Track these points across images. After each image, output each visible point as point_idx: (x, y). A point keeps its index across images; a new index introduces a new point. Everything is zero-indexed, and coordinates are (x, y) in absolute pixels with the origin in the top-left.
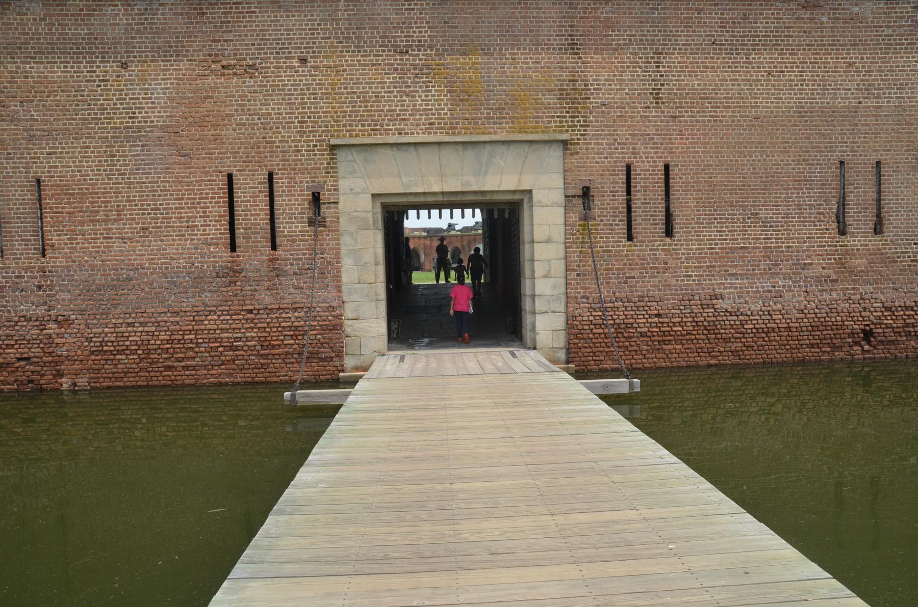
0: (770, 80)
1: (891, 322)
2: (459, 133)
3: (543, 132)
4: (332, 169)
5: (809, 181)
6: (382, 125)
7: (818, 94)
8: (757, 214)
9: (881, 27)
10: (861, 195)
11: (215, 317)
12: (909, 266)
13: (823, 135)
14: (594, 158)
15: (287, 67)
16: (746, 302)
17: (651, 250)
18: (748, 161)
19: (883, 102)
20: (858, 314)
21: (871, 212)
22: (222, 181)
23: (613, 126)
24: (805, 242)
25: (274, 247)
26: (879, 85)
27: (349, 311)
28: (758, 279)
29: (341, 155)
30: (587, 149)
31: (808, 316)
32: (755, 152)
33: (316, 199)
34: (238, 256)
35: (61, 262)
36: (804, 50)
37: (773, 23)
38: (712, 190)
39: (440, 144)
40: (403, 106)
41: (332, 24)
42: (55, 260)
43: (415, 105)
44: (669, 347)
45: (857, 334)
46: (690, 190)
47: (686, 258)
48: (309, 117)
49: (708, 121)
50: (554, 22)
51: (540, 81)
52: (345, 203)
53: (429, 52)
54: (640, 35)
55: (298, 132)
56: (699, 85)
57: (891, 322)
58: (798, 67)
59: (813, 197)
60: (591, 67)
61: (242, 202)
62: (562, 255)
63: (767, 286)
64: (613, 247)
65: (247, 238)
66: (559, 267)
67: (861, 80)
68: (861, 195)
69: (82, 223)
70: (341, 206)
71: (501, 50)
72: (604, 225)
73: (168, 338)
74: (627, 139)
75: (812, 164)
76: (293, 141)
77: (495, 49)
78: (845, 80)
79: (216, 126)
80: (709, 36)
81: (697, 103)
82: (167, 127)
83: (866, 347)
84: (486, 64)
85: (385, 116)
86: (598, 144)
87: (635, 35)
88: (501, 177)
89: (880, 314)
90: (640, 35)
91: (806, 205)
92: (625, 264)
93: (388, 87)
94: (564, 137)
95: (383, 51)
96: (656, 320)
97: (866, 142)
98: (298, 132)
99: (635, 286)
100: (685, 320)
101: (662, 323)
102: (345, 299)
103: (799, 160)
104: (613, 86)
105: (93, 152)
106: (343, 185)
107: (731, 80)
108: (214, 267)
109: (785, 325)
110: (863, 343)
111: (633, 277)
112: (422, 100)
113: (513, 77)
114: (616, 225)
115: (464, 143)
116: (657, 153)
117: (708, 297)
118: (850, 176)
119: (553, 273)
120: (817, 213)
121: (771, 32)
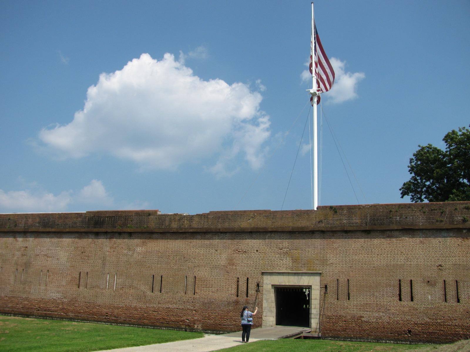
0: (378, 257)
1: (417, 328)
2: (294, 270)
3: (315, 270)
5: (389, 285)
6: (275, 268)
7: (392, 260)
8: (374, 294)
9: (411, 242)
10: (406, 289)
11: (232, 313)
12: (422, 311)
13: (394, 272)
14: (328, 277)
15: (253, 252)
16: (371, 319)
17: (343, 303)
18: (371, 279)
19: (412, 263)
20: (406, 325)
21: (409, 294)
22: (236, 279)
23: (333, 269)
24: (388, 303)
25: (247, 296)
26: (411, 258)
27: (264, 314)
28: (374, 313)
30: (326, 275)
31: (390, 324)
32: (373, 277)
33: (258, 285)
34: (238, 298)
35: (198, 296)
36: (388, 248)
37: (379, 241)
38: (361, 287)
39: (289, 273)
40: (280, 263)
41: (264, 242)
42: (197, 296)
43: (283, 263)
44: (348, 330)
45: (406, 331)
46: (354, 287)
47: (353, 306)
48: (258, 265)
49: (360, 268)
50: (319, 242)
51: (315, 257)
53: (287, 249)
54: (341, 245)
55: (255, 268)
56: (358, 258)
57: (417, 328)
58: (386, 253)
59: (391, 290)
60: (328, 253)
61: (241, 285)
63: (377, 315)
64: (333, 301)
65: (241, 294)
66: (318, 306)
67: (405, 257)
68: (406, 289)
70: (264, 287)
71: (305, 249)
72: (331, 295)
73: (220, 317)
74: (337, 273)
75: (391, 280)
76: (253, 271)
77: (304, 249)
78: (400, 257)
79: (236, 266)
80: (361, 245)
81: (357, 263)
82: (225, 265)
83: (409, 335)
84: (301, 252)
85: (276, 265)
86: (329, 274)
87: (340, 245)
88: (303, 281)
89: (413, 325)
90: (341, 245)
91: (389, 292)
92: (336, 306)
93: (277, 258)
95: (276, 249)
96: (344, 322)
97: (407, 274)
98: (255, 268)
99: (338, 313)
100: (352, 323)
101: (346, 323)
102: (263, 311)
103: (386, 279)
104: (334, 259)
105: (208, 271)
106: (265, 282)
107: (367, 257)
108: (233, 300)
109: (383, 327)
110: (408, 334)
111: (338, 310)
112: (285, 262)
113: (308, 256)
114: (334, 296)
115: (295, 273)
116: (345, 276)
117: (359, 317)
119: (316, 307)
120: (392, 294)
121: (378, 243)
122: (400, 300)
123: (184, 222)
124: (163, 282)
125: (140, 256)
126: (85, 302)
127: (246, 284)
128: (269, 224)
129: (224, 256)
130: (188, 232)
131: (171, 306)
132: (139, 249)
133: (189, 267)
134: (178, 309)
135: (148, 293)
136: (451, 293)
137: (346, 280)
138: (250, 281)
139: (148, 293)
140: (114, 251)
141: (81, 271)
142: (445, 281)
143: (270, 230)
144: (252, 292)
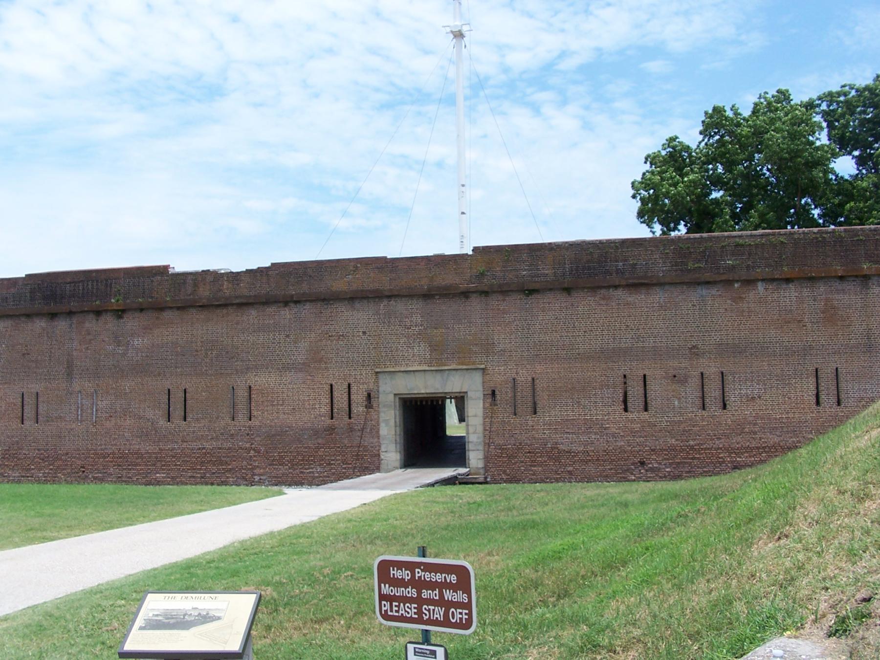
4: (377, 382)
10: (635, 392)
22: (328, 388)
25: (350, 418)
27: (383, 449)
29: (380, 376)
33: (369, 395)
35: (257, 423)
39: (425, 371)
42: (255, 422)
52: (382, 398)
62: (482, 422)
65: (338, 414)
66: (480, 429)
68: (635, 392)
69: (267, 406)
79: (326, 363)
88: (454, 384)
94: (483, 366)
106: (381, 389)
118: (629, 382)
122: (626, 410)
123: (223, 285)
124: (189, 402)
125: (140, 354)
126: (39, 450)
127: (346, 395)
128: (385, 283)
129: (303, 345)
130: (232, 305)
131: (207, 445)
132: (137, 342)
133: (237, 370)
134: (220, 448)
135: (161, 423)
136: (712, 392)
137: (530, 379)
138: (354, 389)
139: (161, 423)
140: (87, 349)
141: (25, 390)
142: (702, 374)
143: (387, 294)
144: (359, 409)
